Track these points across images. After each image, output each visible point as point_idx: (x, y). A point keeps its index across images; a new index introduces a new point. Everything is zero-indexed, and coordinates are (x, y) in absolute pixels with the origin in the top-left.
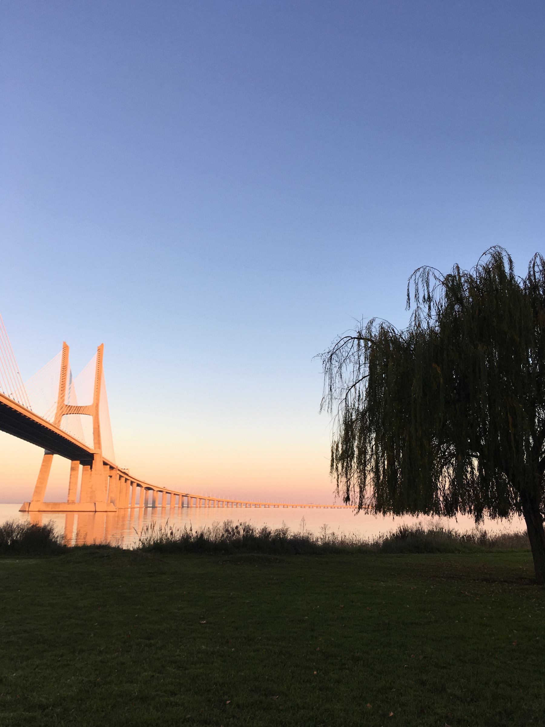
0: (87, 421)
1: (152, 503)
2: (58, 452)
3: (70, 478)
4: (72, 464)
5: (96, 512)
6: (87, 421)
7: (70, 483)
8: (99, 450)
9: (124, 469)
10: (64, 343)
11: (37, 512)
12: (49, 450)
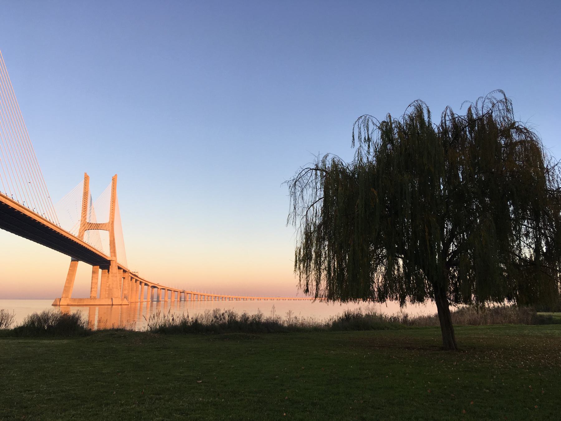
0: (104, 235)
1: (157, 298)
2: (81, 259)
3: (92, 280)
4: (93, 268)
5: (113, 305)
6: (104, 235)
7: (92, 283)
8: (114, 257)
9: (135, 272)
10: (86, 174)
11: (66, 306)
12: (74, 258)
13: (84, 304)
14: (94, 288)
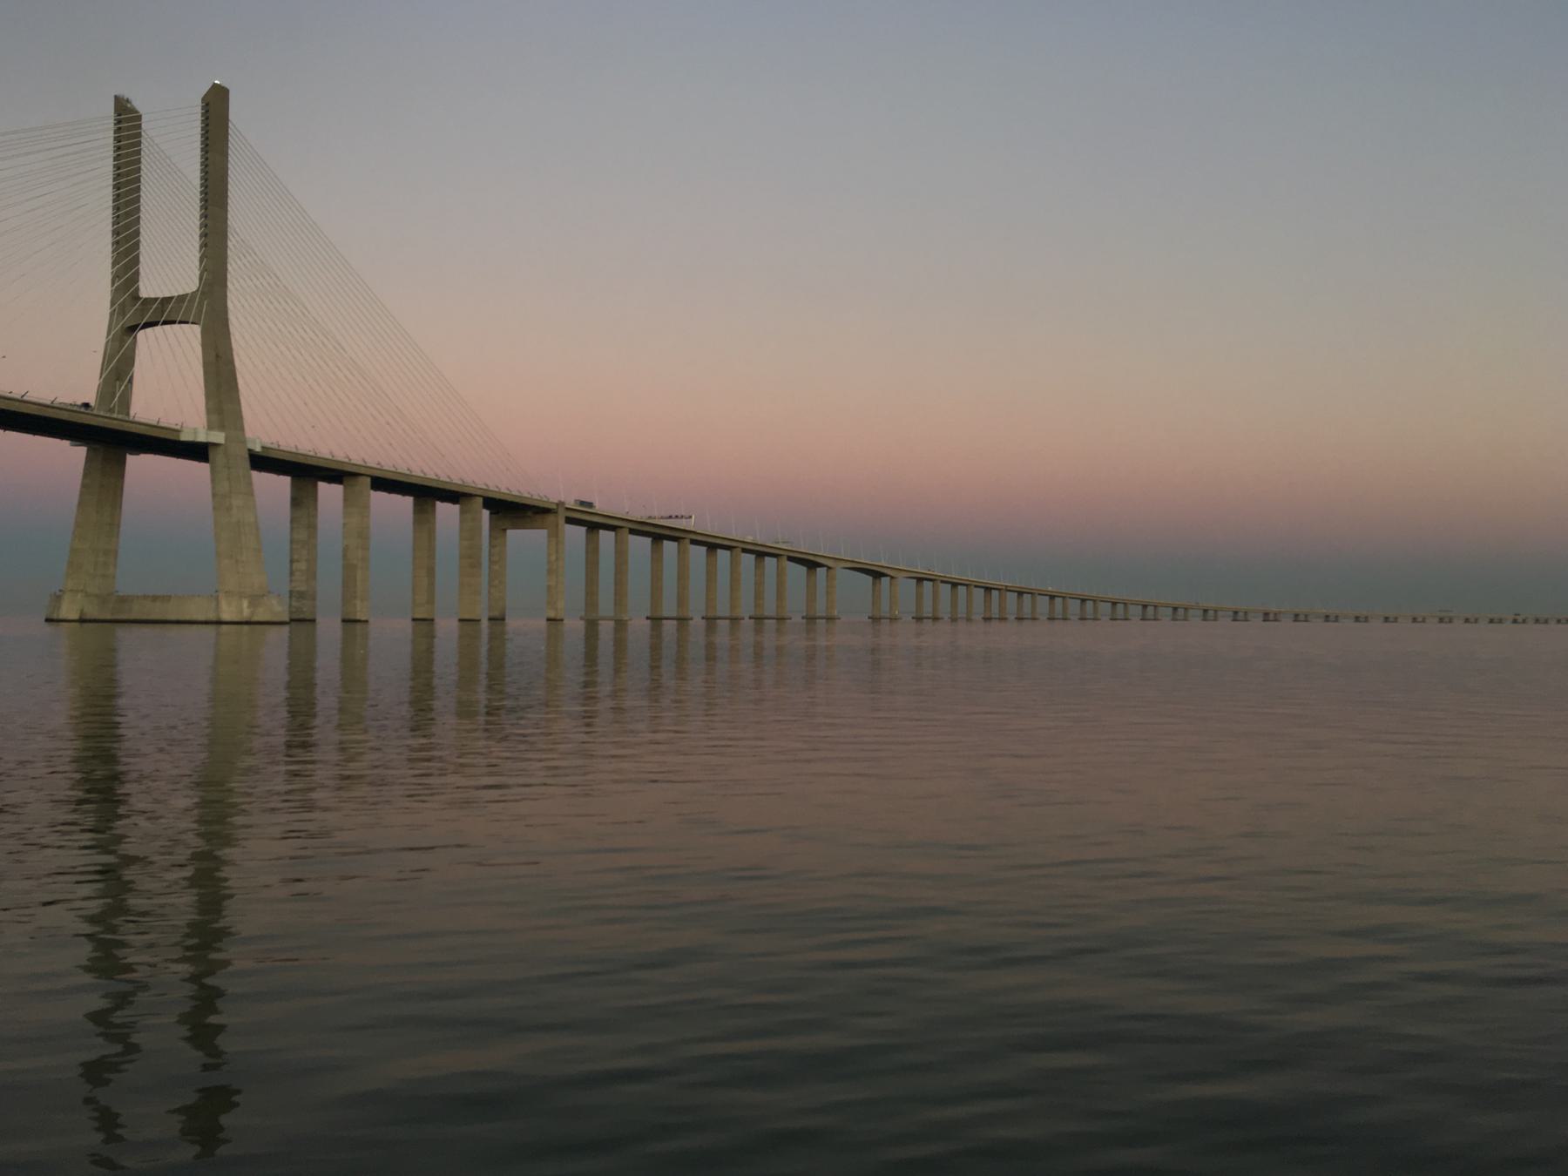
3: (292, 529)
11: (77, 624)
13: (132, 617)
14: (298, 561)
